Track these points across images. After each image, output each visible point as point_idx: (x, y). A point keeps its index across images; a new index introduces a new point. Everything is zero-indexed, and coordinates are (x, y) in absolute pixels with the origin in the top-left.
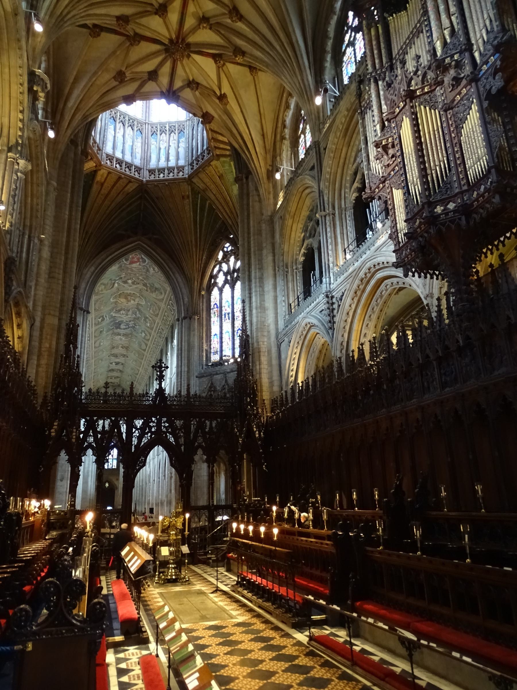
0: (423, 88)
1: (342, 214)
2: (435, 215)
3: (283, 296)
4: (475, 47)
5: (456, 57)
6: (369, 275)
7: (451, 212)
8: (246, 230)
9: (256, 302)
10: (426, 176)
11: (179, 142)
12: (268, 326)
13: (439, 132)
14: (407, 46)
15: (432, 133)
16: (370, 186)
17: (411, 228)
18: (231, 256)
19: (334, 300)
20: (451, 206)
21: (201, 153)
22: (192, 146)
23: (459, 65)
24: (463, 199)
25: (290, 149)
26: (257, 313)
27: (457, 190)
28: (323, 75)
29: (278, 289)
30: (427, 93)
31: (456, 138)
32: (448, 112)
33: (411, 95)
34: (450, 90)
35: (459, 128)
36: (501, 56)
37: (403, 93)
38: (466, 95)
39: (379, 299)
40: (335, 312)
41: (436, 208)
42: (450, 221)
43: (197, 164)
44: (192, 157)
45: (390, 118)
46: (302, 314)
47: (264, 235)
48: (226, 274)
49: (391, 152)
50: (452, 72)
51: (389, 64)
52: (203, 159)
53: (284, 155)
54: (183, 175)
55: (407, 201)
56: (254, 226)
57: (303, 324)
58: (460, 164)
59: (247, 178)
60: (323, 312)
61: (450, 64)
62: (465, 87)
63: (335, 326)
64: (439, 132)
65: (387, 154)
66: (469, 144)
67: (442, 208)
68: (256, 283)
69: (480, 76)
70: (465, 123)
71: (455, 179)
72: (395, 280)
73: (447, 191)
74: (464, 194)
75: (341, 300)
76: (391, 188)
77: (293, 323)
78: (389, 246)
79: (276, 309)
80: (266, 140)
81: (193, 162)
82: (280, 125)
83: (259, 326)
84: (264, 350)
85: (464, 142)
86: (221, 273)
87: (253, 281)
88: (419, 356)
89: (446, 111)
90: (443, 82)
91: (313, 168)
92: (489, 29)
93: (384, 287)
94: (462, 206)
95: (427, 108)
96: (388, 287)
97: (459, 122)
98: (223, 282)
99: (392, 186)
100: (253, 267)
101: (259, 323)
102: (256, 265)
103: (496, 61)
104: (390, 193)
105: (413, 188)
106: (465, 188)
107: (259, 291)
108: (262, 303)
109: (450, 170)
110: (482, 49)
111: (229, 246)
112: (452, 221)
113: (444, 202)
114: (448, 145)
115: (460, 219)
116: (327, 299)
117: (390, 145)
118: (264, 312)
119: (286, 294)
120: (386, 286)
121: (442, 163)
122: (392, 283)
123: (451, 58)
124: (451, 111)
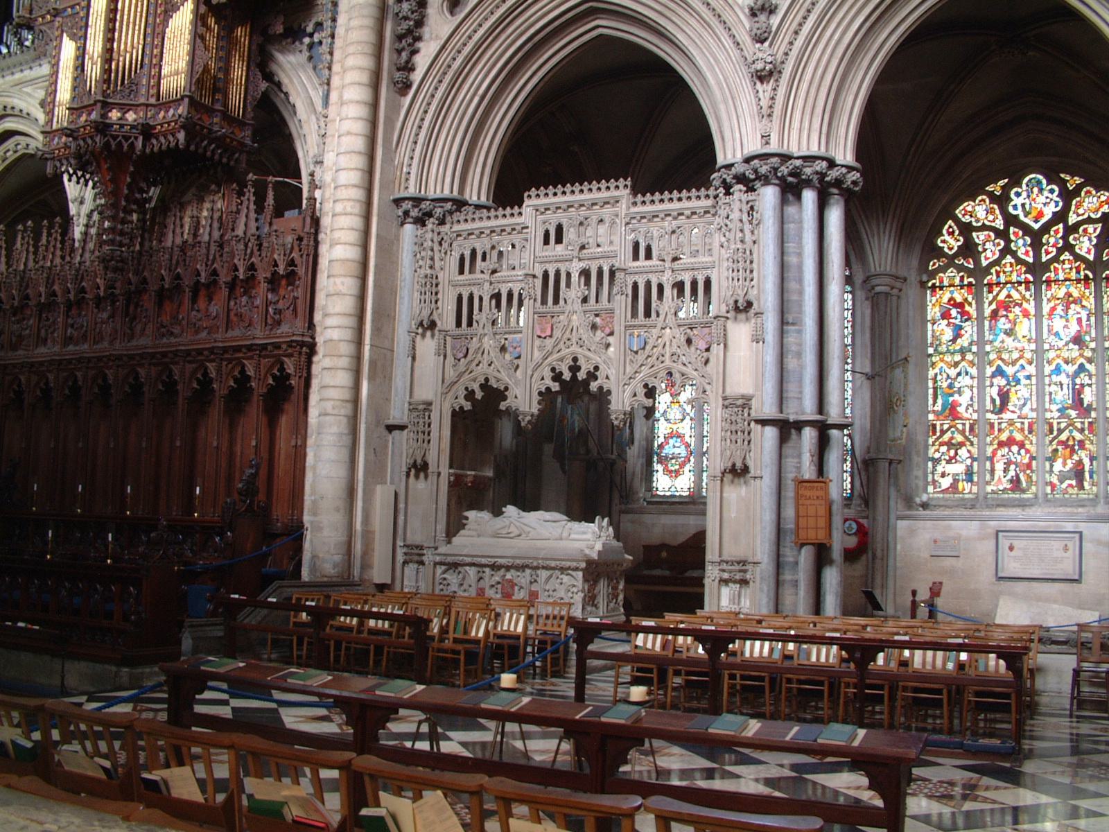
20: (131, 116)
27: (142, 100)
31: (161, 26)
41: (110, 111)
67: (119, 115)
76: (62, 32)
88: (42, 289)
93: (13, 145)
96: (19, 147)
97: (169, 6)
99: (65, 29)
106: (153, 101)
109: (142, 67)
112: (127, 138)
113: (124, 108)
114: (149, 31)
115: (136, 138)
120: (16, 145)
121: (135, 51)
122: (28, 145)
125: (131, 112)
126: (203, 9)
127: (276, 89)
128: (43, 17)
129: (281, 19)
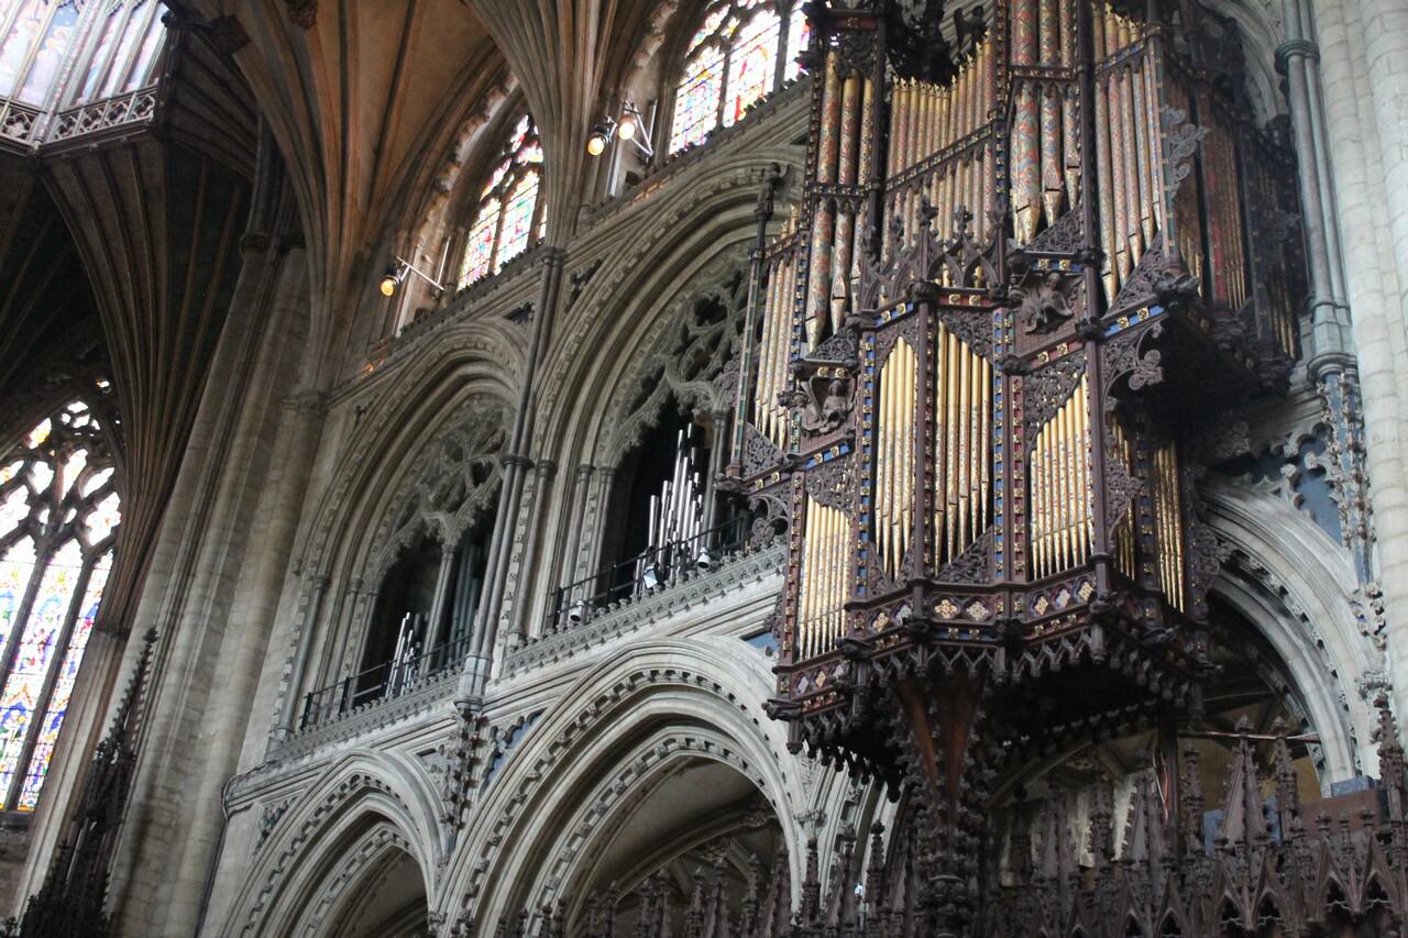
0: (965, 295)
1: (575, 484)
2: (935, 620)
3: (291, 661)
4: (1108, 265)
5: (1063, 265)
6: (625, 695)
7: (974, 627)
8: (225, 407)
9: (189, 649)
10: (931, 511)
11: (48, 33)
12: (204, 743)
13: (980, 416)
14: (932, 169)
15: (963, 409)
16: (741, 462)
17: (859, 629)
18: (77, 447)
19: (485, 733)
20: (978, 612)
21: (115, 98)
22: (91, 62)
23: (1063, 286)
24: (1011, 606)
25: (443, 223)
26: (180, 686)
27: (1000, 579)
28: (626, 85)
29: (278, 631)
30: (972, 310)
31: (1021, 448)
32: (1013, 378)
33: (932, 299)
34: (1029, 329)
35: (1030, 430)
36: (1167, 315)
37: (918, 285)
38: (1064, 358)
39: (633, 775)
40: (479, 771)
41: (938, 603)
42: (967, 650)
43: (87, 123)
44: (79, 93)
45: (862, 326)
46: (352, 742)
47: (281, 445)
48: (36, 501)
49: (832, 403)
50: (1046, 293)
51: (876, 185)
52: (113, 117)
53: (424, 235)
54: (23, 136)
55: (864, 554)
56: (257, 407)
57: (344, 776)
58: (1018, 515)
59: (283, 251)
60: (430, 759)
61: (1046, 275)
62: (1069, 340)
63: (468, 816)
64: (980, 416)
65: (820, 404)
66: (1051, 476)
67: (955, 609)
68: (206, 586)
69: (1108, 334)
70: (1049, 421)
71: (1001, 549)
72: (700, 735)
73: (974, 570)
74: (1016, 594)
75: (509, 740)
77: (306, 760)
78: (717, 633)
79: (249, 692)
80: (382, 168)
81: (75, 112)
82: (438, 147)
83: (173, 733)
84: (165, 820)
85: (1036, 466)
86: (23, 492)
87: (200, 578)
89: (1008, 372)
90: (1019, 303)
91: (520, 315)
92: (1148, 245)
93: (660, 744)
94: (1008, 623)
95: (964, 346)
96: (671, 747)
97: (1034, 412)
98: (16, 525)
100: (212, 533)
101: (179, 722)
102: (224, 528)
103: (1152, 319)
104: (800, 507)
105: (886, 527)
106: (1021, 580)
107: (211, 617)
108: (209, 659)
109: (990, 521)
110: (1123, 276)
111: (82, 413)
112: (974, 654)
115: (992, 652)
116: (462, 723)
117: (834, 386)
118: (206, 692)
119: (301, 656)
122: (688, 741)
123: (1050, 262)
124: (1020, 378)
125: (978, 605)
128: (766, 477)
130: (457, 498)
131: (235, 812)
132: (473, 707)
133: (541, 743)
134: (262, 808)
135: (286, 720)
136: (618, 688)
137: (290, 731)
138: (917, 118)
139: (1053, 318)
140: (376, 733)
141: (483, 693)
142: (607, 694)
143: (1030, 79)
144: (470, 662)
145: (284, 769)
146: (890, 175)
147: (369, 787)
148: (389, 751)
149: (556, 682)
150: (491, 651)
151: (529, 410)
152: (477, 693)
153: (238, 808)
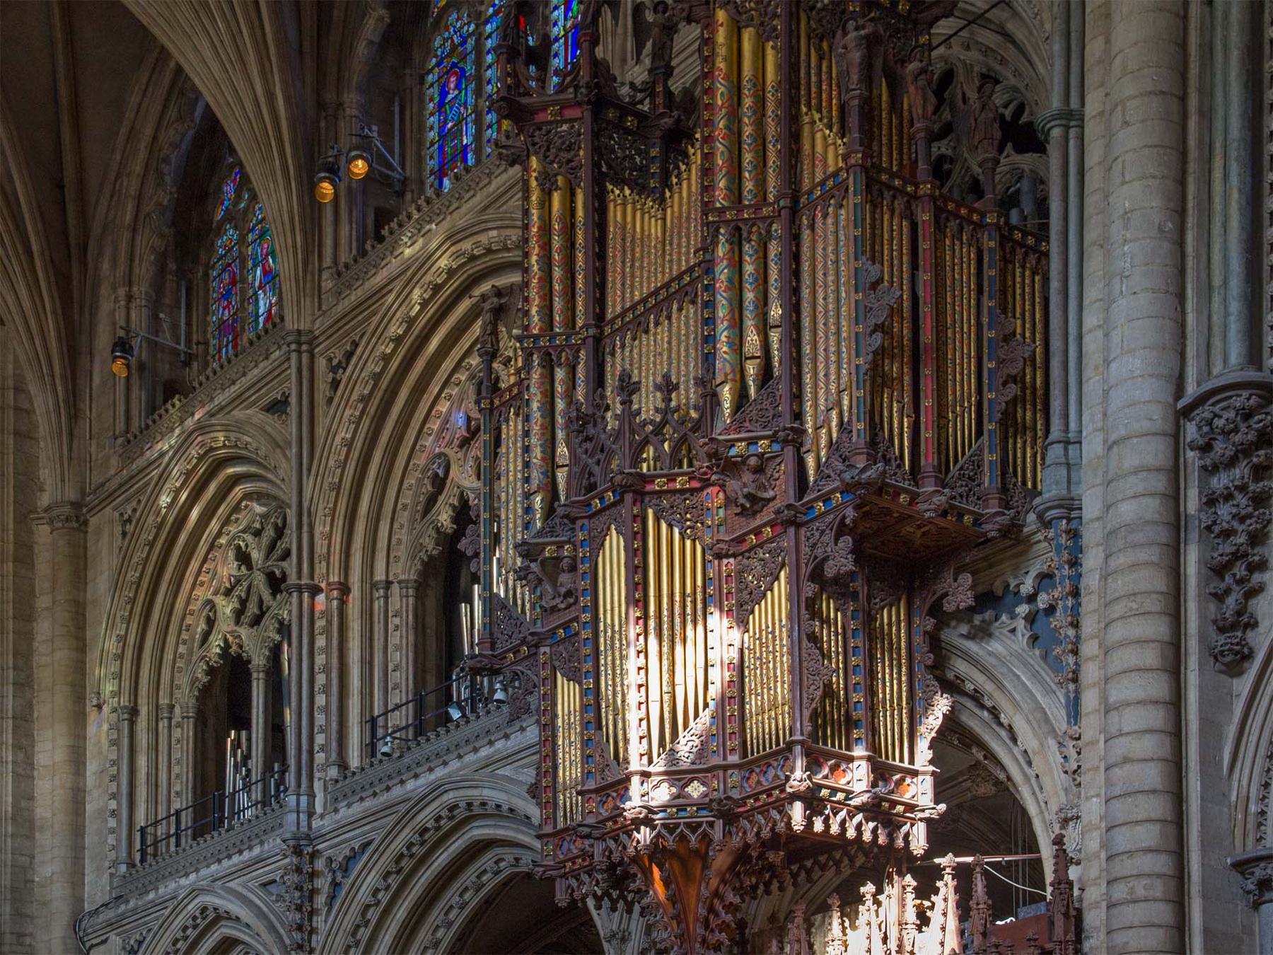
6: (446, 825)
38: (770, 540)
50: (747, 477)
75: (345, 870)
78: (522, 767)
126: (809, 589)
127: (970, 704)
129: (966, 579)
130: (256, 611)
131: (92, 946)
132: (302, 842)
133: (373, 873)
134: (119, 940)
135: (124, 854)
136: (438, 819)
137: (132, 865)
138: (633, 241)
139: (755, 503)
140: (214, 867)
141: (310, 827)
142: (429, 825)
143: (727, 222)
144: (292, 800)
145: (132, 904)
146: (609, 316)
147: (220, 917)
148: (231, 885)
149: (378, 816)
150: (311, 786)
151: (305, 528)
152: (304, 829)
153: (94, 942)
